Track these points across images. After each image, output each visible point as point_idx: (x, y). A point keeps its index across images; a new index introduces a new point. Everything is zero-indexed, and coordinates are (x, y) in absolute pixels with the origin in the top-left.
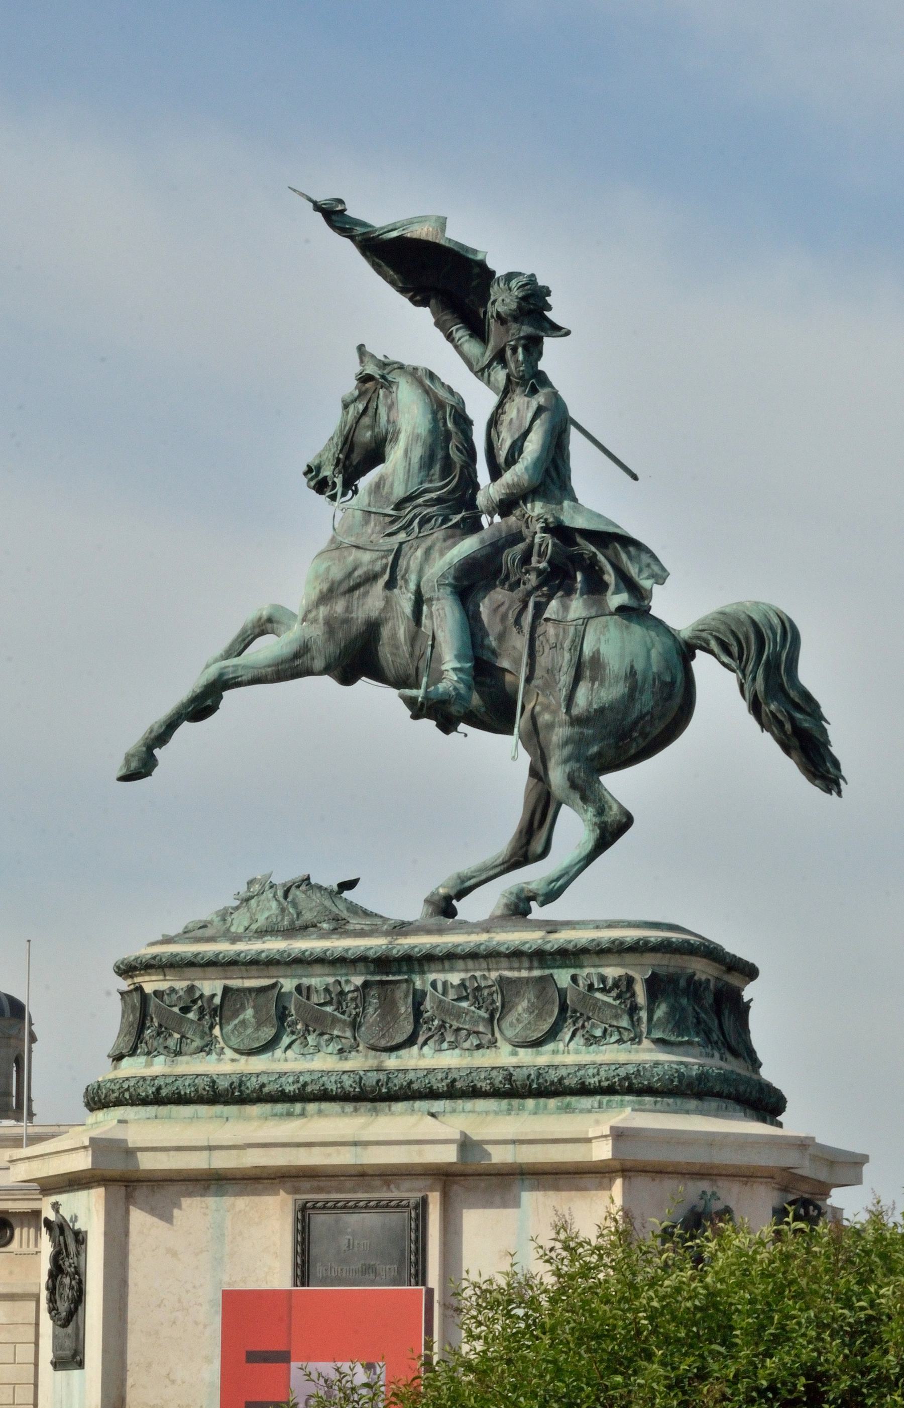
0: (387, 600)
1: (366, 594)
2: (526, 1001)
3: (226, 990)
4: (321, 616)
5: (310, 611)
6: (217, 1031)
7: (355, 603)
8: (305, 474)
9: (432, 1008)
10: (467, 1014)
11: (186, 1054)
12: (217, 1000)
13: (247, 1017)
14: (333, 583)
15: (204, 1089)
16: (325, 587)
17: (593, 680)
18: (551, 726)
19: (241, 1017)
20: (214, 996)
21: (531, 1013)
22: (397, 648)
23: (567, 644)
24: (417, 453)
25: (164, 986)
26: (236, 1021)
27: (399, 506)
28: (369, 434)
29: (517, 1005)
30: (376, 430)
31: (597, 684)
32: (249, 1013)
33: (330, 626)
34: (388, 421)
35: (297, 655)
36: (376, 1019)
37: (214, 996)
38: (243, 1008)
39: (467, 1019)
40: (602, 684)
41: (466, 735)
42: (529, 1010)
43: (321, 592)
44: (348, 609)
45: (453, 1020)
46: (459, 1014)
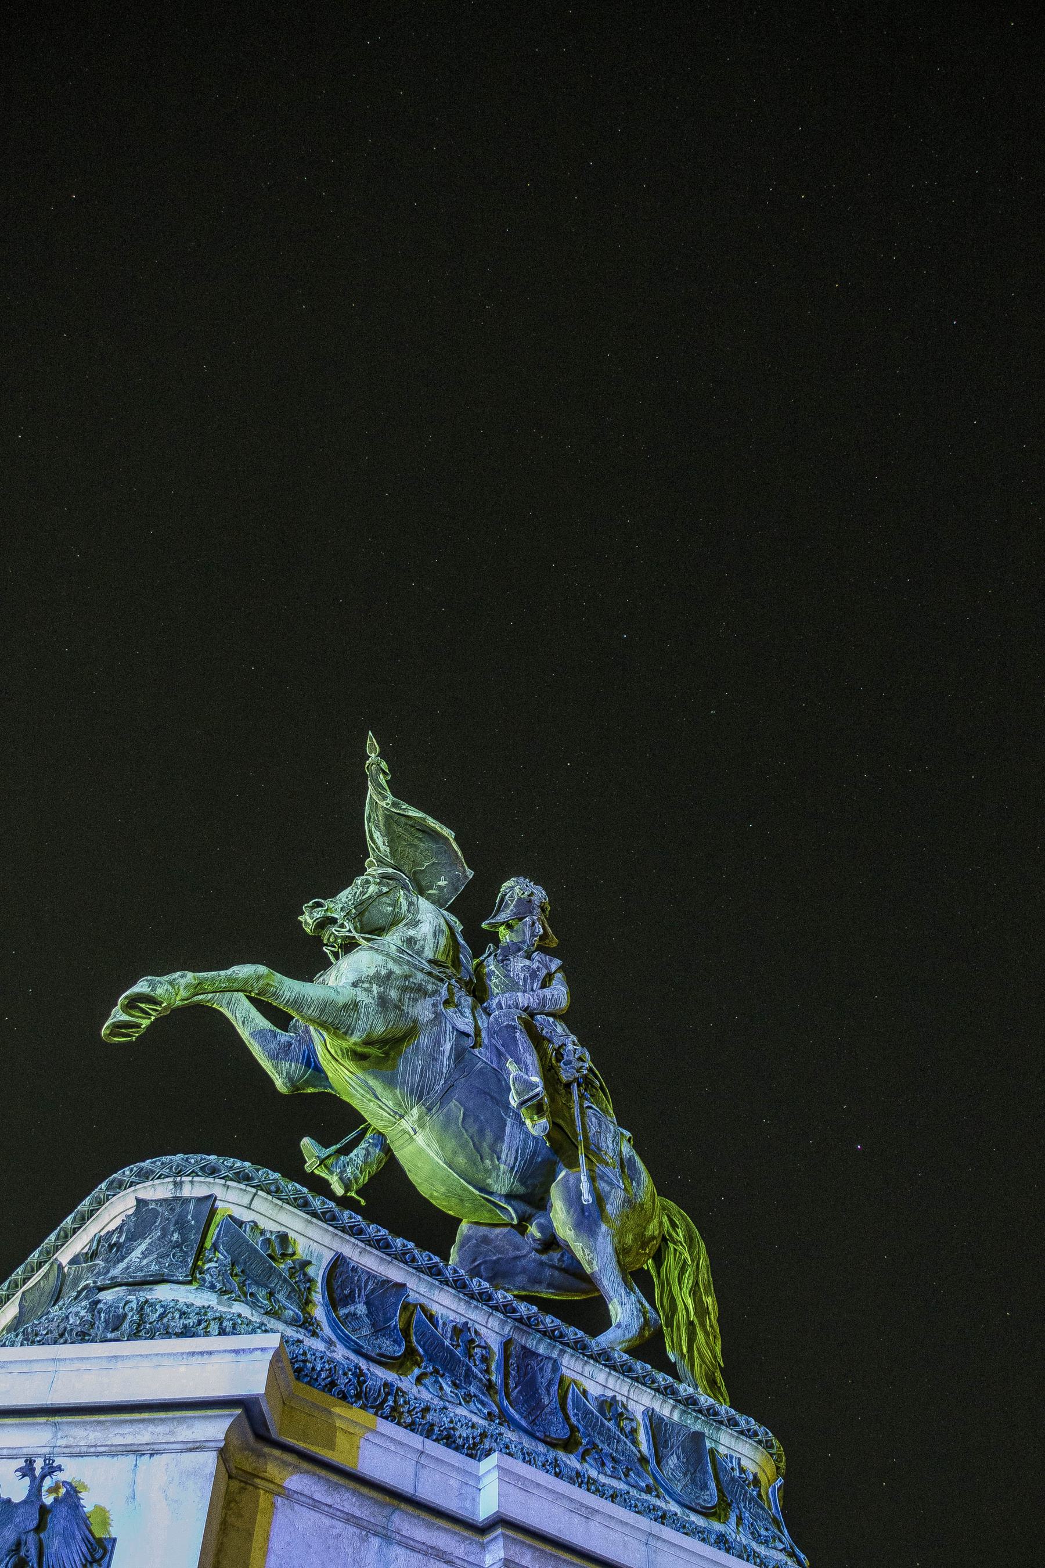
1: (416, 1000)
3: (339, 1262)
5: (363, 982)
12: (317, 1273)
14: (391, 973)
15: (345, 1374)
16: (384, 972)
20: (309, 1263)
24: (443, 941)
25: (246, 1216)
30: (397, 910)
32: (361, 1309)
33: (383, 1002)
35: (345, 1006)
37: (309, 1263)
43: (378, 973)
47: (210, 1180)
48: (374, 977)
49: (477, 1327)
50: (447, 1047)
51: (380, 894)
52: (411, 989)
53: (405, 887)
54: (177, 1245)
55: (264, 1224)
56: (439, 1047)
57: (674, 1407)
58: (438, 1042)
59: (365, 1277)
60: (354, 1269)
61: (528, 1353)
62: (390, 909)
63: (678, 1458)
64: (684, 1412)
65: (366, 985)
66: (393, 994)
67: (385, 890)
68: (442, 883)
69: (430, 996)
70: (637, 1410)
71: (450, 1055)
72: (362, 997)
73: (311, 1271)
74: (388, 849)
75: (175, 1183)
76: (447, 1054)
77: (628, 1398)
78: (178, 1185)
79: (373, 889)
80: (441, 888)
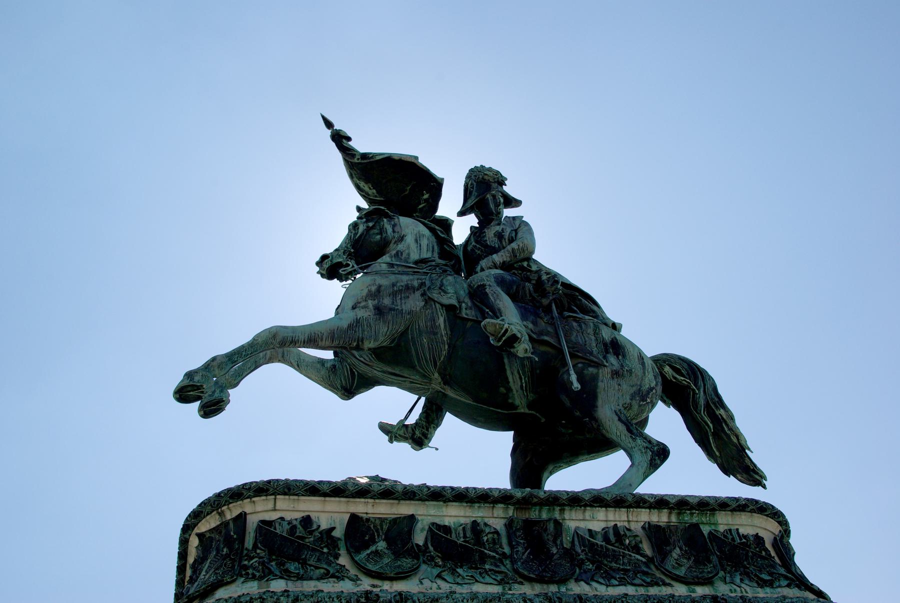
0: (428, 301)
2: (678, 549)
3: (354, 519)
4: (371, 306)
6: (343, 560)
7: (399, 301)
8: (318, 264)
9: (582, 551)
10: (623, 557)
11: (311, 579)
12: (338, 533)
13: (380, 548)
16: (373, 288)
17: (617, 354)
18: (595, 378)
19: (373, 548)
20: (333, 529)
21: (689, 559)
22: (435, 334)
23: (590, 331)
25: (273, 516)
26: (369, 552)
27: (416, 263)
28: (378, 237)
29: (671, 552)
30: (384, 235)
31: (620, 357)
32: (381, 545)
33: (379, 311)
34: (394, 232)
35: (350, 326)
36: (528, 557)
37: (333, 529)
38: (373, 541)
39: (626, 561)
40: (624, 356)
41: (437, 449)
42: (685, 555)
43: (370, 291)
44: (393, 303)
45: (611, 562)
46: (615, 557)
47: (240, 502)
48: (367, 295)
49: (486, 520)
50: (441, 321)
51: (368, 229)
52: (400, 291)
53: (387, 216)
54: (228, 556)
55: (288, 516)
56: (435, 323)
57: (670, 513)
58: (433, 320)
59: (378, 522)
60: (368, 520)
61: (529, 524)
62: (378, 237)
63: (681, 549)
64: (679, 514)
65: (363, 304)
66: (387, 301)
67: (371, 224)
68: (426, 196)
69: (418, 290)
70: (636, 527)
71: (445, 326)
72: (360, 313)
73: (334, 534)
74: (374, 191)
75: (219, 514)
76: (442, 326)
77: (629, 521)
78: (221, 514)
79: (361, 228)
80: (426, 200)
